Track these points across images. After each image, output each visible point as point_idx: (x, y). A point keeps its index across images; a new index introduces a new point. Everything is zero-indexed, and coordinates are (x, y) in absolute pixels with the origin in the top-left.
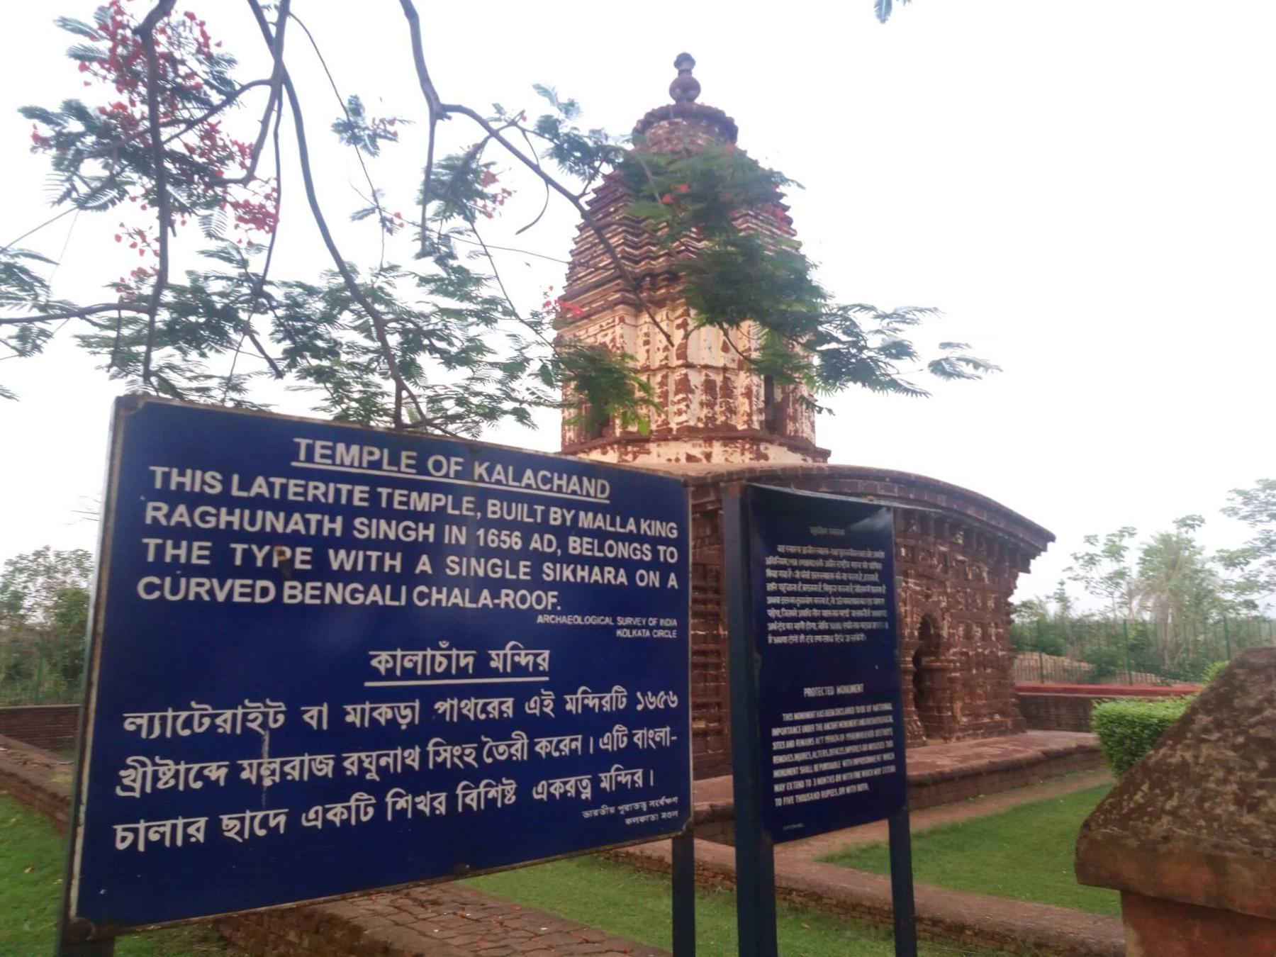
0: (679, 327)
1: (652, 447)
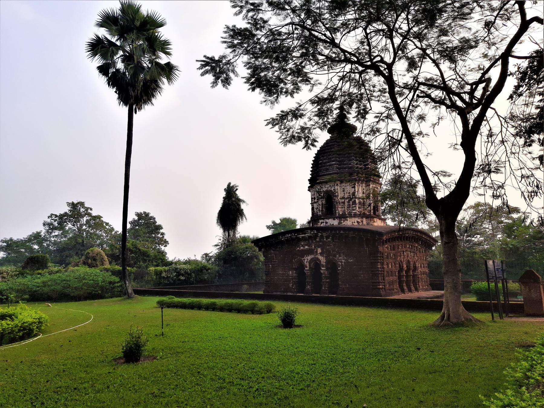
0: (352, 187)
1: (348, 219)
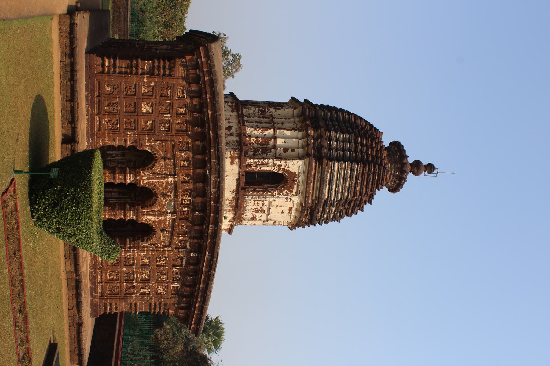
1: (235, 113)
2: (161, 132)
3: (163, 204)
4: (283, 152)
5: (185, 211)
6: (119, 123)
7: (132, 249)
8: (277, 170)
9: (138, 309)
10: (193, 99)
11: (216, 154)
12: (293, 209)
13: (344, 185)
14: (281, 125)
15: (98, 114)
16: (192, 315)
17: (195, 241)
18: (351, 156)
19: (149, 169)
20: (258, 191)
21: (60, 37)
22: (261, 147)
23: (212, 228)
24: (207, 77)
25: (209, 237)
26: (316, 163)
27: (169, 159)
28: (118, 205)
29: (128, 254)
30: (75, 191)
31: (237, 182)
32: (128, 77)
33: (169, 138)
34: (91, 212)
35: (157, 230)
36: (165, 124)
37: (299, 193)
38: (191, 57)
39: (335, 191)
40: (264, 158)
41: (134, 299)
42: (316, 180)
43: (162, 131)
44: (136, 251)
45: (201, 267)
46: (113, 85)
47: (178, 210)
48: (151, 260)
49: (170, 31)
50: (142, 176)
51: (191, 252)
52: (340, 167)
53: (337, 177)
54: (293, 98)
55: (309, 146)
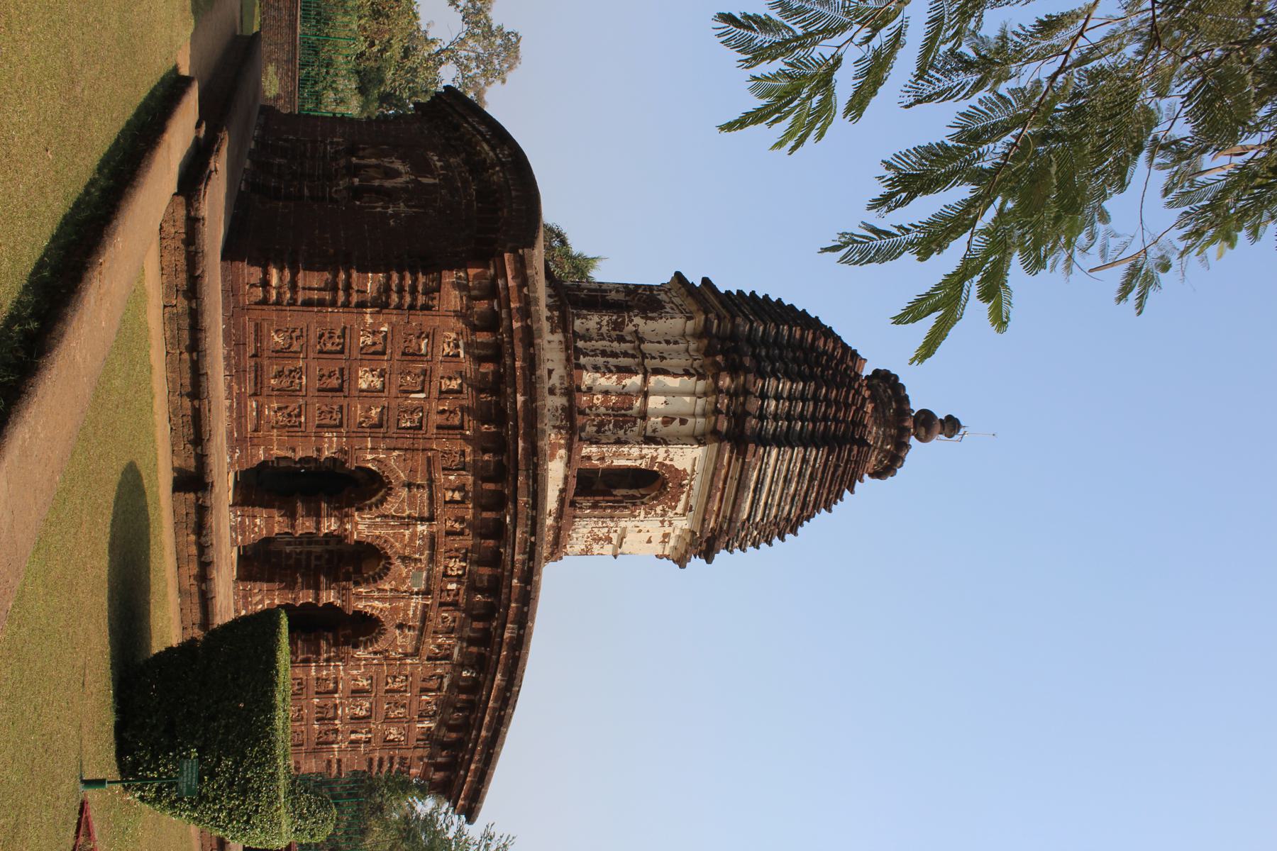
1: (558, 337)
2: (403, 431)
3: (404, 575)
4: (661, 425)
5: (453, 590)
6: (303, 412)
7: (333, 664)
8: (646, 466)
9: (343, 768)
10: (479, 366)
11: (528, 485)
12: (672, 535)
13: (785, 491)
14: (658, 360)
15: (255, 394)
16: (461, 781)
17: (474, 649)
18: (805, 430)
19: (374, 509)
20: (601, 507)
21: (163, 249)
22: (614, 415)
23: (513, 629)
24: (517, 322)
25: (505, 647)
26: (731, 452)
27: (418, 486)
28: (302, 576)
29: (325, 673)
30: (237, 764)
31: (559, 496)
32: (327, 312)
33: (420, 444)
34: (276, 811)
35: (390, 626)
36: (411, 414)
37: (691, 510)
38: (479, 270)
39: (766, 503)
40: (619, 442)
41: (336, 753)
42: (727, 486)
43: (404, 428)
44: (341, 668)
45: (483, 698)
46: (290, 330)
47: (436, 588)
48: (374, 681)
49: (384, 24)
50: (357, 524)
51: (462, 666)
52: (780, 457)
53: (773, 477)
54: (678, 276)
55: (720, 416)
